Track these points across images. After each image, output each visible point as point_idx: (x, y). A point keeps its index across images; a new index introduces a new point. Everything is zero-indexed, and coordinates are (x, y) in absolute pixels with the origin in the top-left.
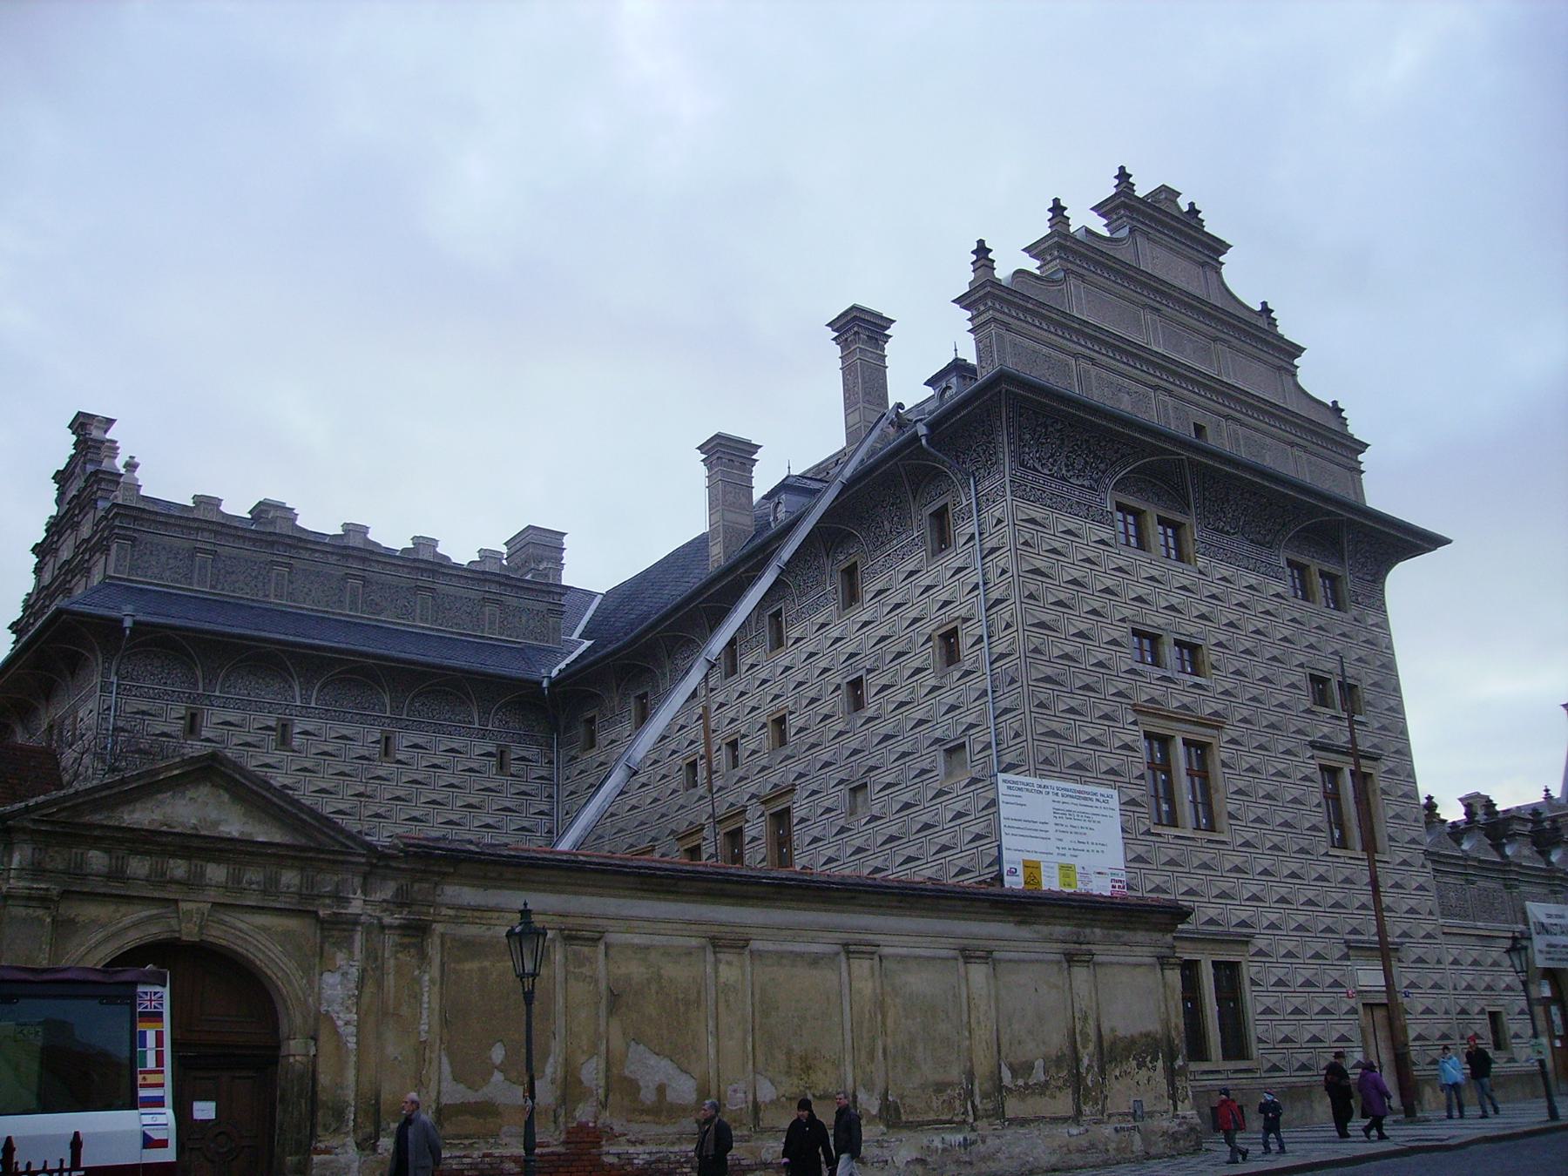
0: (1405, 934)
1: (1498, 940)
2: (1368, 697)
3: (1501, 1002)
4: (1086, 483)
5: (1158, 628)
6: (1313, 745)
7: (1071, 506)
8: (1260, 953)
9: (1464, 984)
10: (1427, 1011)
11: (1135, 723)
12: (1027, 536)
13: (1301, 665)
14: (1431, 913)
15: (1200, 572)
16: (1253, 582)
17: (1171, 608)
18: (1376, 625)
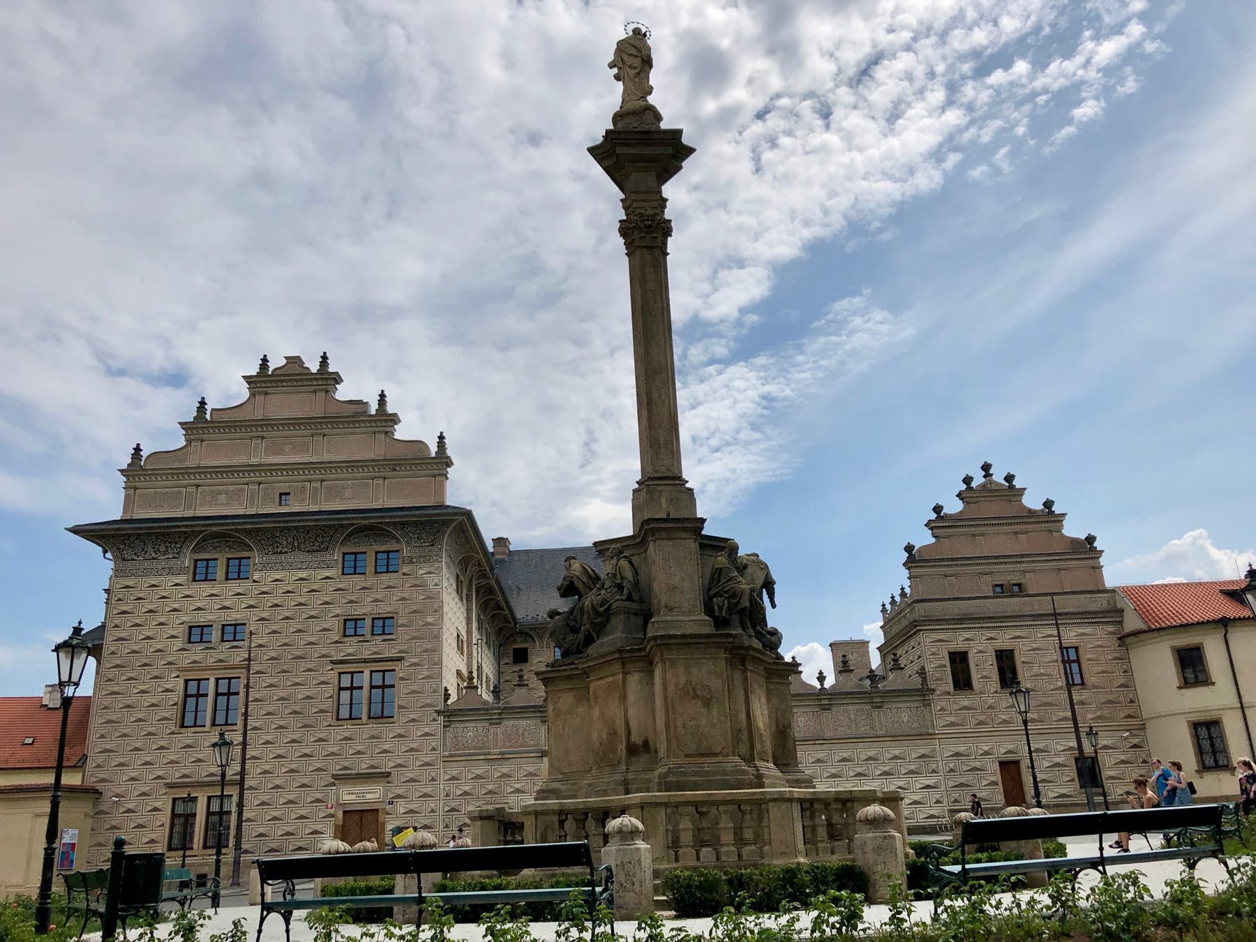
0: (400, 765)
2: (400, 622)
3: (505, 801)
4: (171, 556)
5: (210, 621)
6: (332, 662)
7: (157, 572)
9: (459, 792)
10: (411, 811)
11: (178, 677)
12: (120, 596)
13: (337, 616)
14: (434, 749)
15: (254, 581)
16: (303, 574)
17: (224, 608)
18: (429, 573)
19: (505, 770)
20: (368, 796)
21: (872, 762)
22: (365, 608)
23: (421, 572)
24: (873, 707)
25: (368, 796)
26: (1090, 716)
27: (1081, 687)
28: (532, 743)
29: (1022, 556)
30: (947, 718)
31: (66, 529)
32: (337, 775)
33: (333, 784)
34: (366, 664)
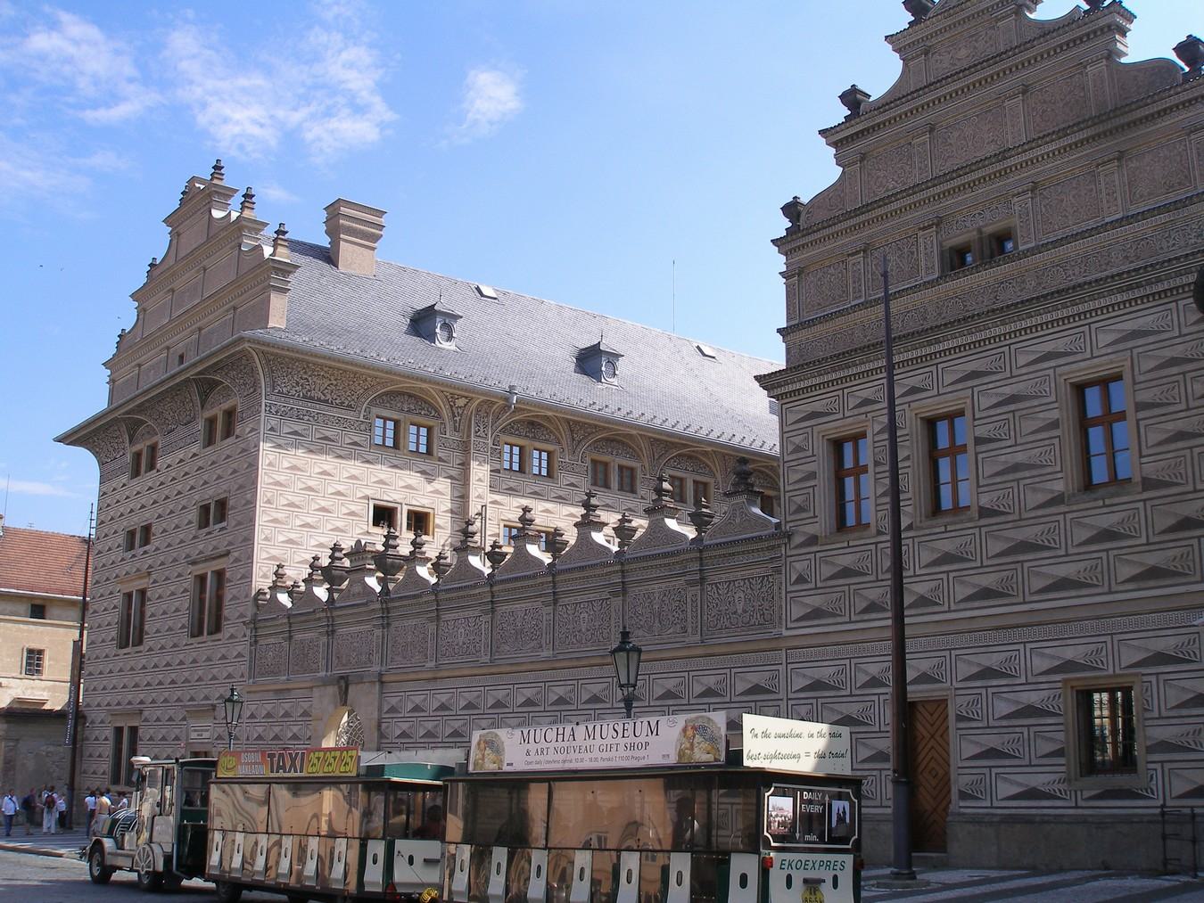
1: (294, 692)
4: (121, 453)
8: (146, 720)
19: (287, 706)
20: (206, 735)
21: (670, 702)
22: (210, 494)
23: (248, 430)
24: (691, 583)
25: (206, 735)
26: (1126, 572)
27: (1112, 489)
28: (315, 666)
29: (1003, 155)
30: (807, 600)
31: (60, 440)
32: (189, 706)
33: (184, 719)
34: (208, 564)
